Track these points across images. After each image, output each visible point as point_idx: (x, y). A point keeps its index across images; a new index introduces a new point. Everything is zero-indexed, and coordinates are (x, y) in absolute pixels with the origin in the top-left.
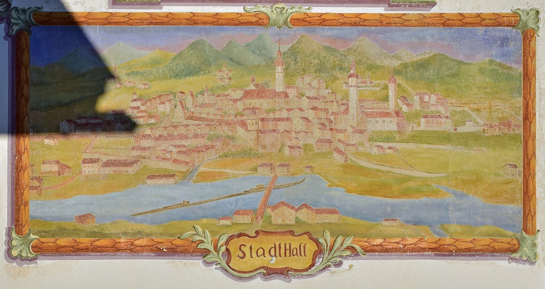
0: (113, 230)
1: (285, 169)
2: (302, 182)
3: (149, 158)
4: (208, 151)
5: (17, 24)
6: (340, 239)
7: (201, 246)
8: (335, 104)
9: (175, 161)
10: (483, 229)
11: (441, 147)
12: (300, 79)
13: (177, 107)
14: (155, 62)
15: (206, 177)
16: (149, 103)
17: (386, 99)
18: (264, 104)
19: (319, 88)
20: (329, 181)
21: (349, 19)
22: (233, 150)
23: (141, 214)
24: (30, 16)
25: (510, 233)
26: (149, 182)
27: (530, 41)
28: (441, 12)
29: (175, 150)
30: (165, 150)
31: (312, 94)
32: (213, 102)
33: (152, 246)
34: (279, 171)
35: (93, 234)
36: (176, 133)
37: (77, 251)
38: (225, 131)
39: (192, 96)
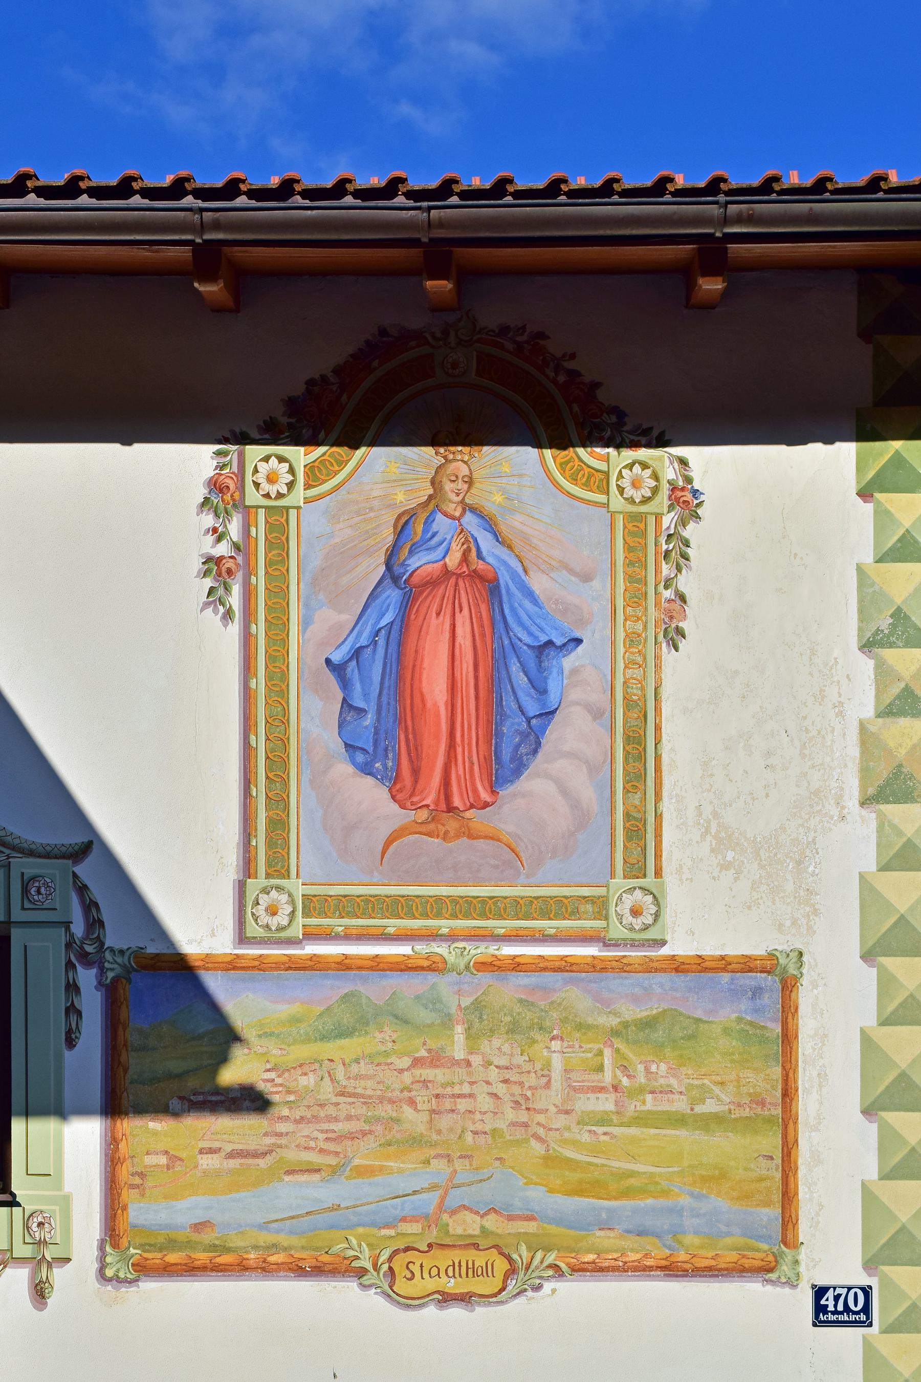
0: (240, 1243)
1: (467, 1162)
2: (489, 1178)
3: (286, 1146)
4: (365, 1138)
5: (112, 970)
6: (539, 1255)
7: (356, 1264)
8: (534, 1075)
9: (322, 1151)
10: (728, 1241)
11: (673, 1132)
12: (486, 1042)
13: (324, 1080)
14: (295, 1020)
15: (363, 1172)
16: (286, 1075)
17: (600, 1068)
18: (438, 1075)
19: (512, 1055)
20: (526, 1178)
21: (552, 963)
22: (398, 1136)
23: (277, 1221)
24: (129, 958)
25: (765, 1247)
26: (287, 1178)
27: (791, 991)
28: (672, 953)
29: (321, 1136)
30: (308, 1136)
31: (503, 1062)
32: (371, 1072)
33: (291, 1263)
34: (459, 1165)
35: (213, 1247)
36: (322, 1114)
37: (192, 1270)
38: (387, 1111)
39: (344, 1065)
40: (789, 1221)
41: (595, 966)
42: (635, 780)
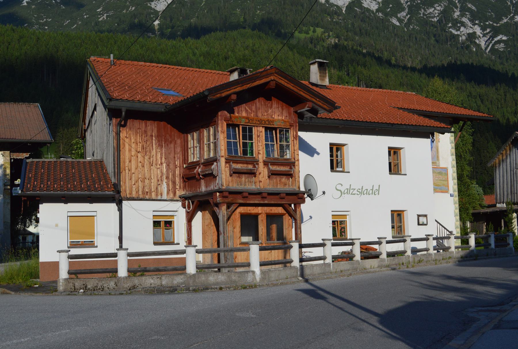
40: (448, 190)
41: (436, 168)
42: (437, 153)
